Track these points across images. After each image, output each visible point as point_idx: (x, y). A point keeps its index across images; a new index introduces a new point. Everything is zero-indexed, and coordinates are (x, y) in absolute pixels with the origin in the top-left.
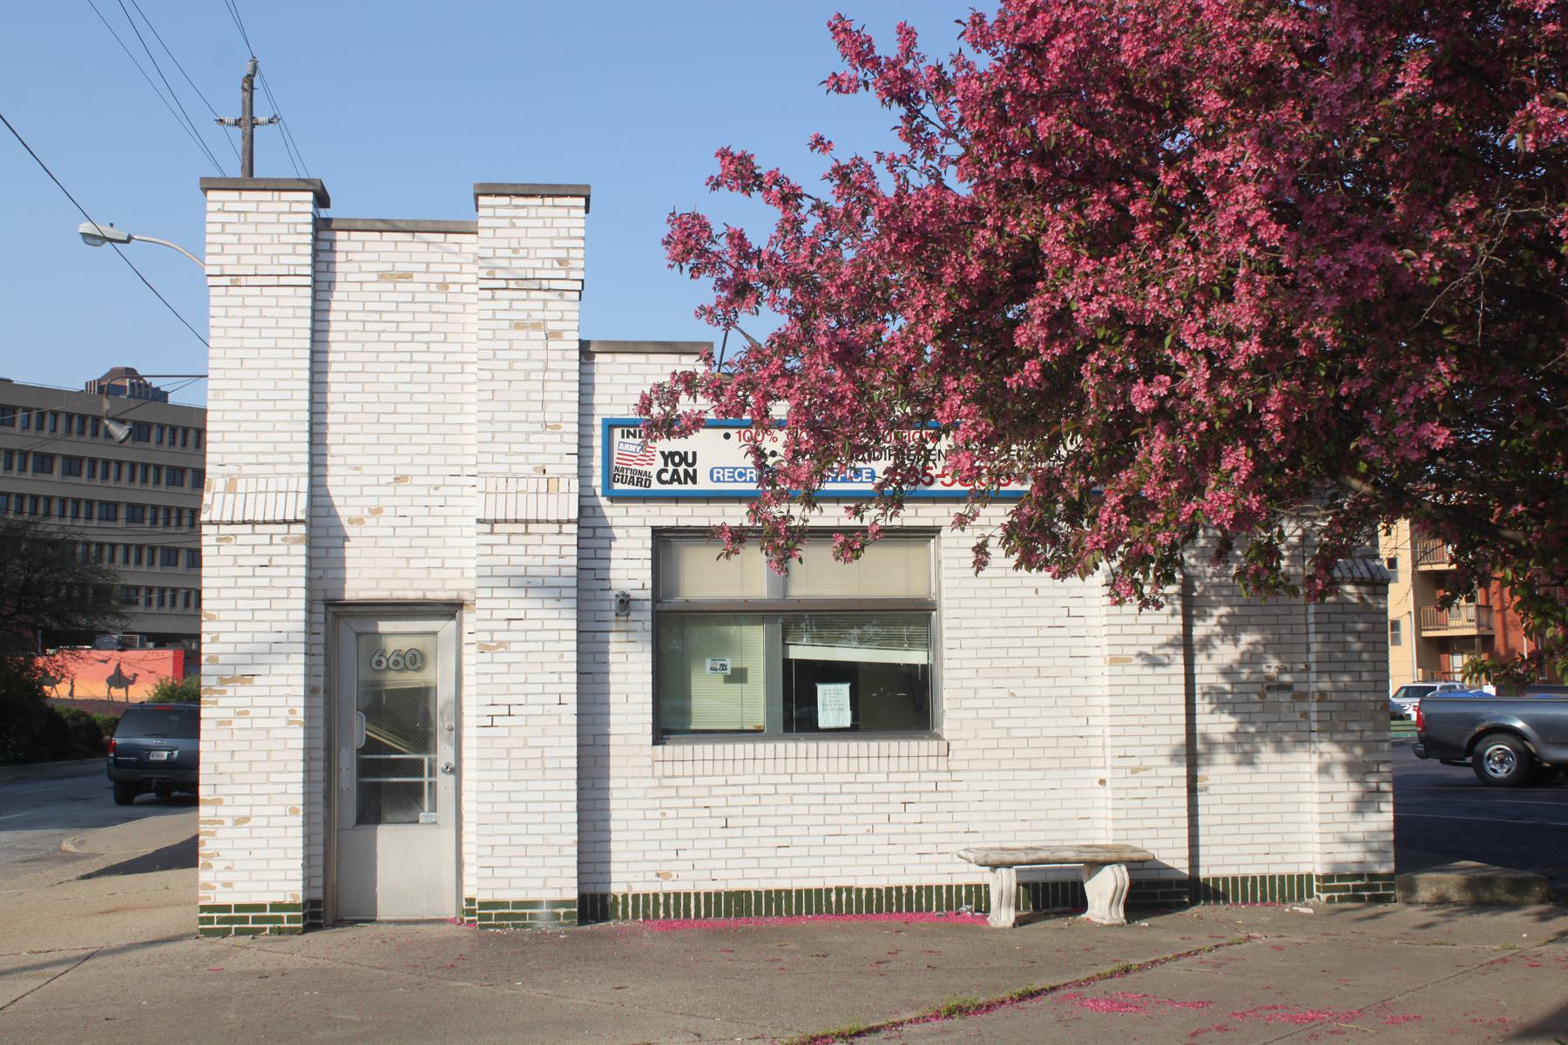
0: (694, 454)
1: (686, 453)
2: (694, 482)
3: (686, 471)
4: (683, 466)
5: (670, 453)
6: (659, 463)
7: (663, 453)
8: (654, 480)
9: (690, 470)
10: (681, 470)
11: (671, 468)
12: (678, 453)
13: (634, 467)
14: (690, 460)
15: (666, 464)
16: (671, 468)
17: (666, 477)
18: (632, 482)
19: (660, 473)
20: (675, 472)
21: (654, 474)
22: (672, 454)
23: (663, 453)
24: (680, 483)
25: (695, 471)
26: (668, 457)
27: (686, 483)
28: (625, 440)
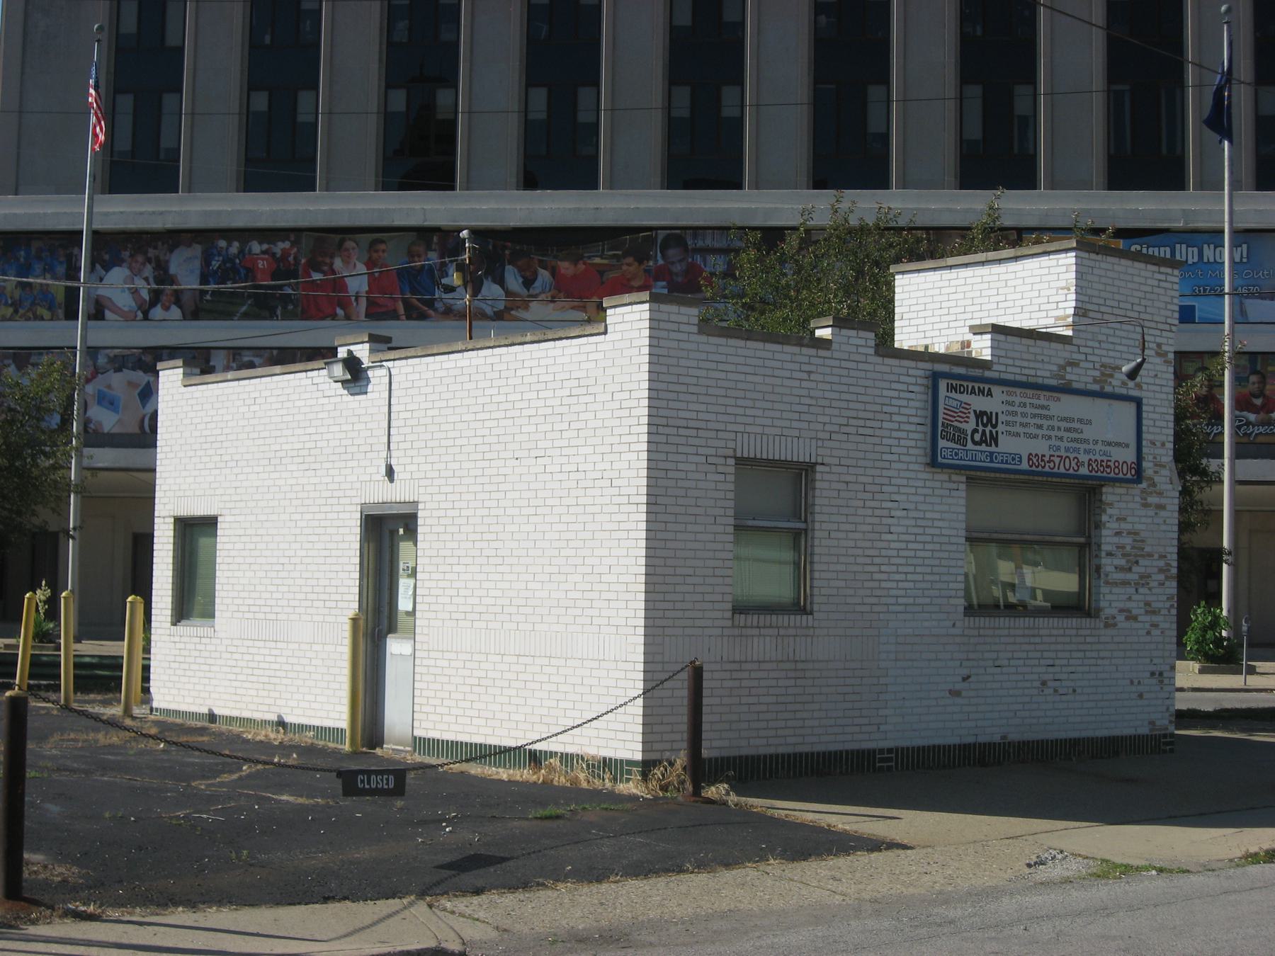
0: (997, 414)
1: (991, 413)
2: (997, 445)
3: (991, 432)
4: (989, 428)
5: (980, 411)
6: (970, 425)
7: (975, 411)
8: (969, 438)
9: (994, 431)
10: (988, 429)
11: (981, 428)
12: (985, 413)
13: (956, 424)
14: (994, 422)
15: (977, 425)
16: (981, 428)
17: (977, 437)
18: (953, 440)
19: (975, 431)
20: (984, 432)
21: (969, 433)
22: (983, 413)
23: (975, 411)
24: (987, 445)
25: (997, 432)
26: (980, 415)
27: (991, 446)
28: (949, 394)
